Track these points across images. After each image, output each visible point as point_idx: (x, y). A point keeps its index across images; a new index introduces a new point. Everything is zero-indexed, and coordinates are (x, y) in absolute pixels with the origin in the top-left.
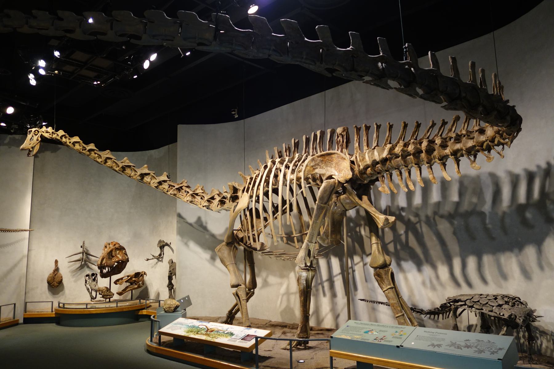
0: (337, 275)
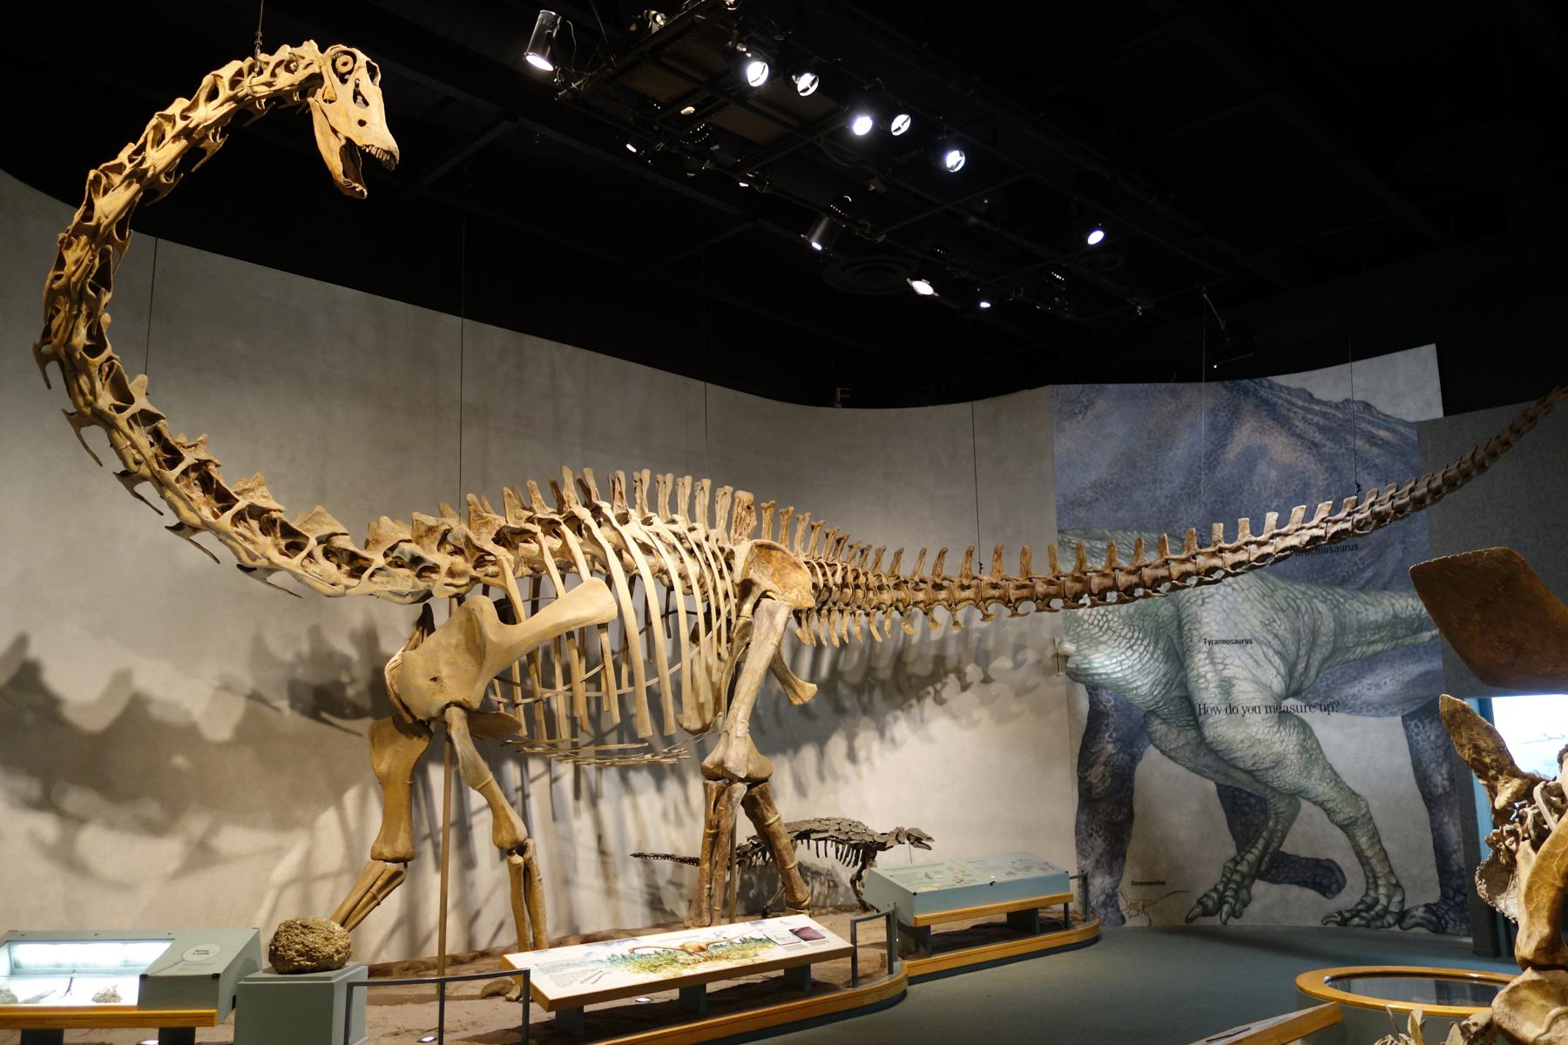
0: (480, 810)
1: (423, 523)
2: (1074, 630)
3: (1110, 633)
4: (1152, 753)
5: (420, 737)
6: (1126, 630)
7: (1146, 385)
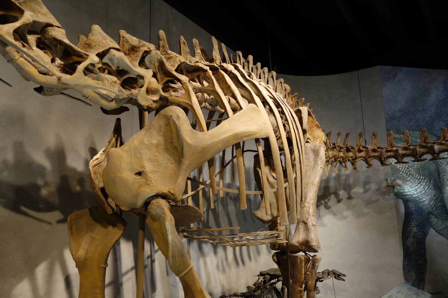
0: (127, 272)
1: (128, 42)
2: (396, 175)
3: (411, 176)
4: (432, 232)
5: (114, 226)
6: (417, 175)
7: (418, 69)
